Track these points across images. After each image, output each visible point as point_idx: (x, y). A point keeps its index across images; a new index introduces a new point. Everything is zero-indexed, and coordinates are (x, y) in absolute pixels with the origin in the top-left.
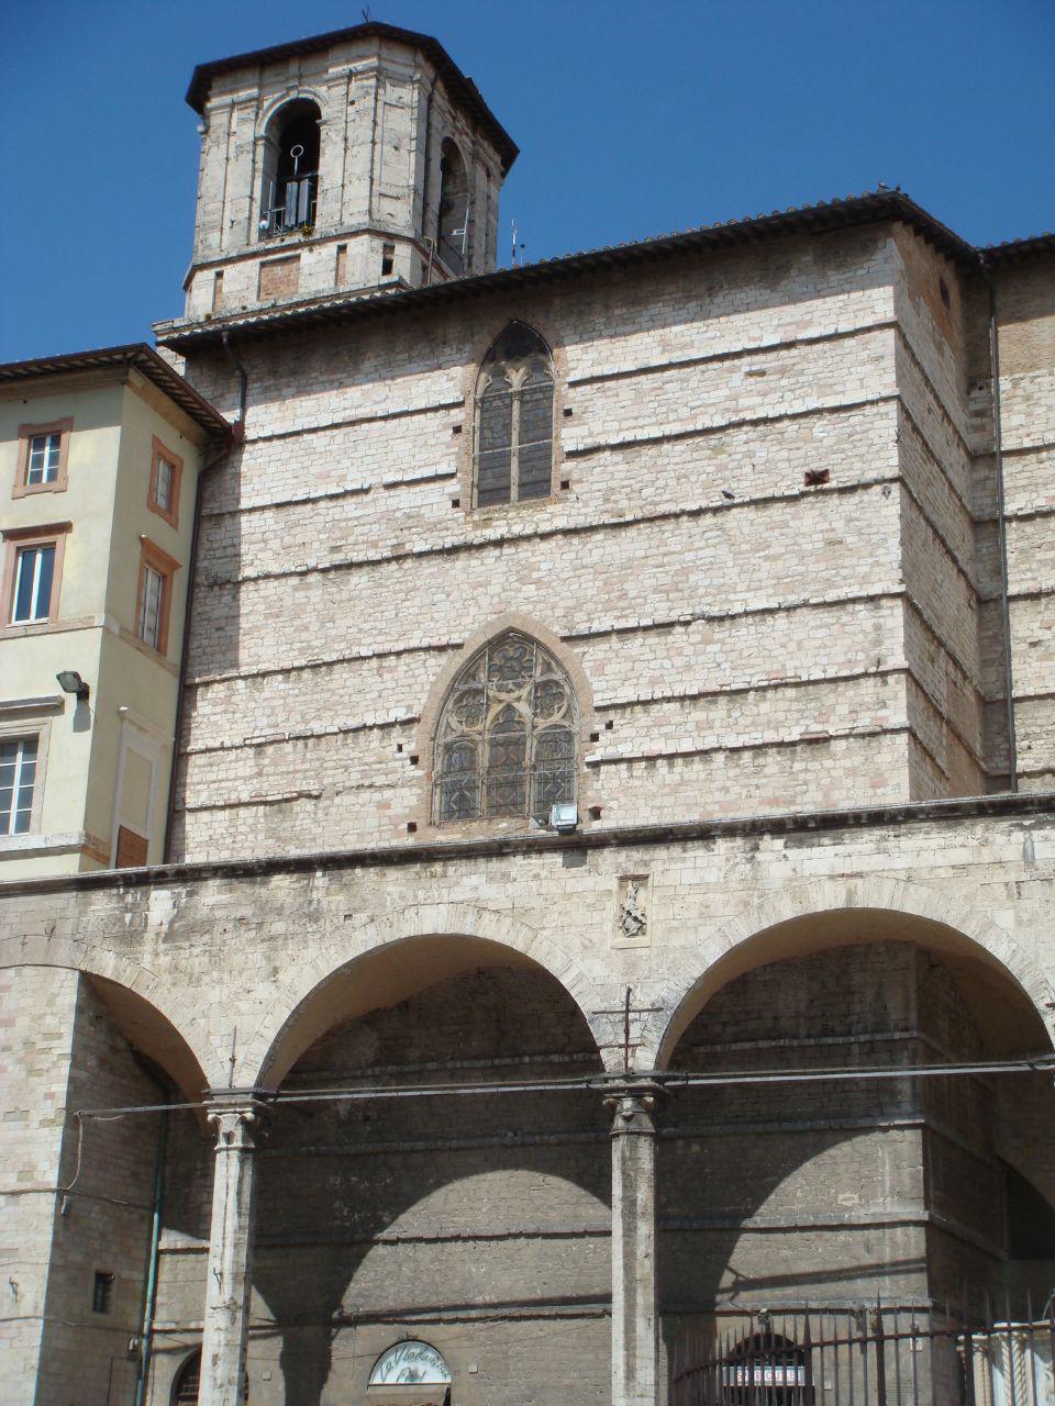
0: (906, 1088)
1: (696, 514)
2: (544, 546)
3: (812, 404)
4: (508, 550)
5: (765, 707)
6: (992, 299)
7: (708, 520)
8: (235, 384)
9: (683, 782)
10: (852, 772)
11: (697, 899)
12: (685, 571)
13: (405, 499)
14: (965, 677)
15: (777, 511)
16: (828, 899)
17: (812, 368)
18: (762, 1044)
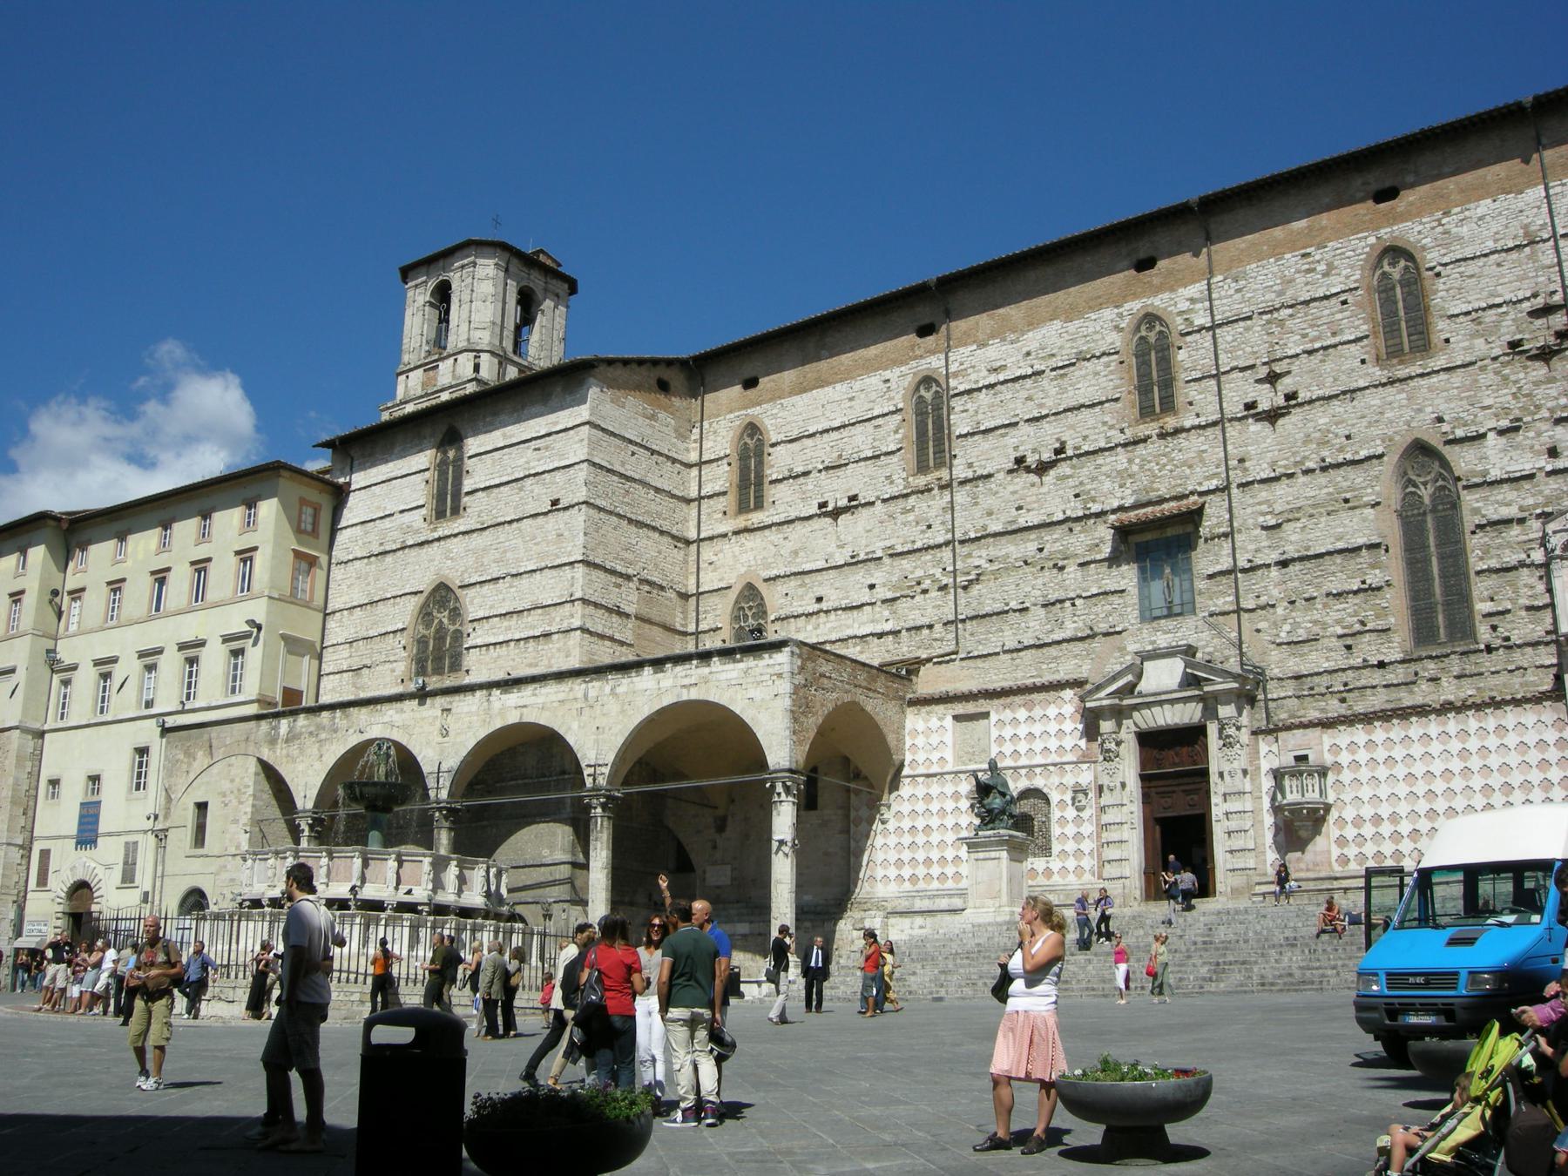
0: (569, 801)
1: (510, 522)
2: (455, 540)
3: (556, 465)
4: (442, 543)
5: (530, 619)
6: (703, 379)
7: (515, 525)
8: (349, 461)
9: (499, 657)
10: (559, 650)
11: (467, 719)
12: (505, 552)
13: (407, 517)
14: (662, 588)
15: (540, 520)
16: (513, 718)
17: (557, 445)
18: (520, 782)
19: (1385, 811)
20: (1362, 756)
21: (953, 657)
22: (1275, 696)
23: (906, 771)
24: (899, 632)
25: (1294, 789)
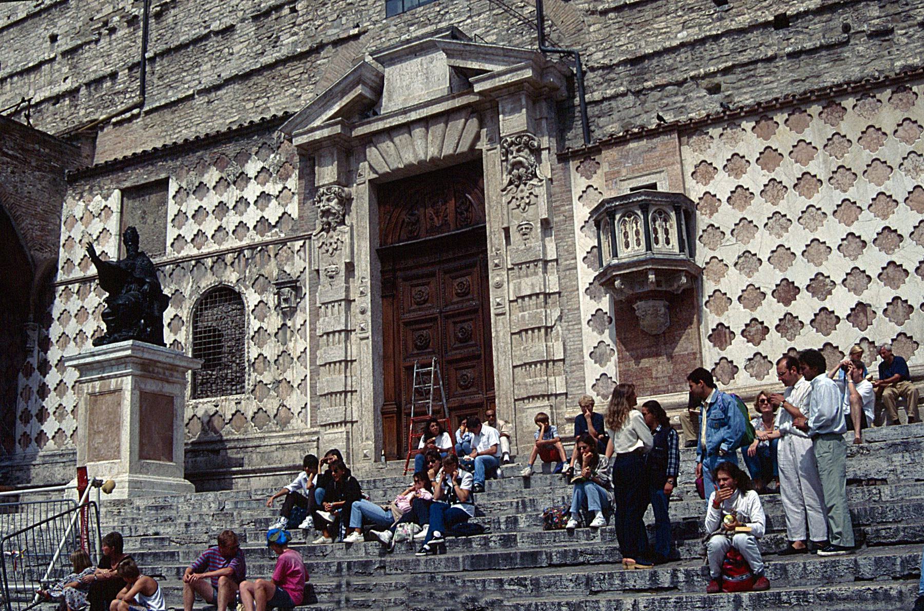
19: (801, 273)
20: (755, 178)
21: (135, 111)
22: (597, 96)
23: (61, 276)
24: (77, 90)
25: (632, 238)
